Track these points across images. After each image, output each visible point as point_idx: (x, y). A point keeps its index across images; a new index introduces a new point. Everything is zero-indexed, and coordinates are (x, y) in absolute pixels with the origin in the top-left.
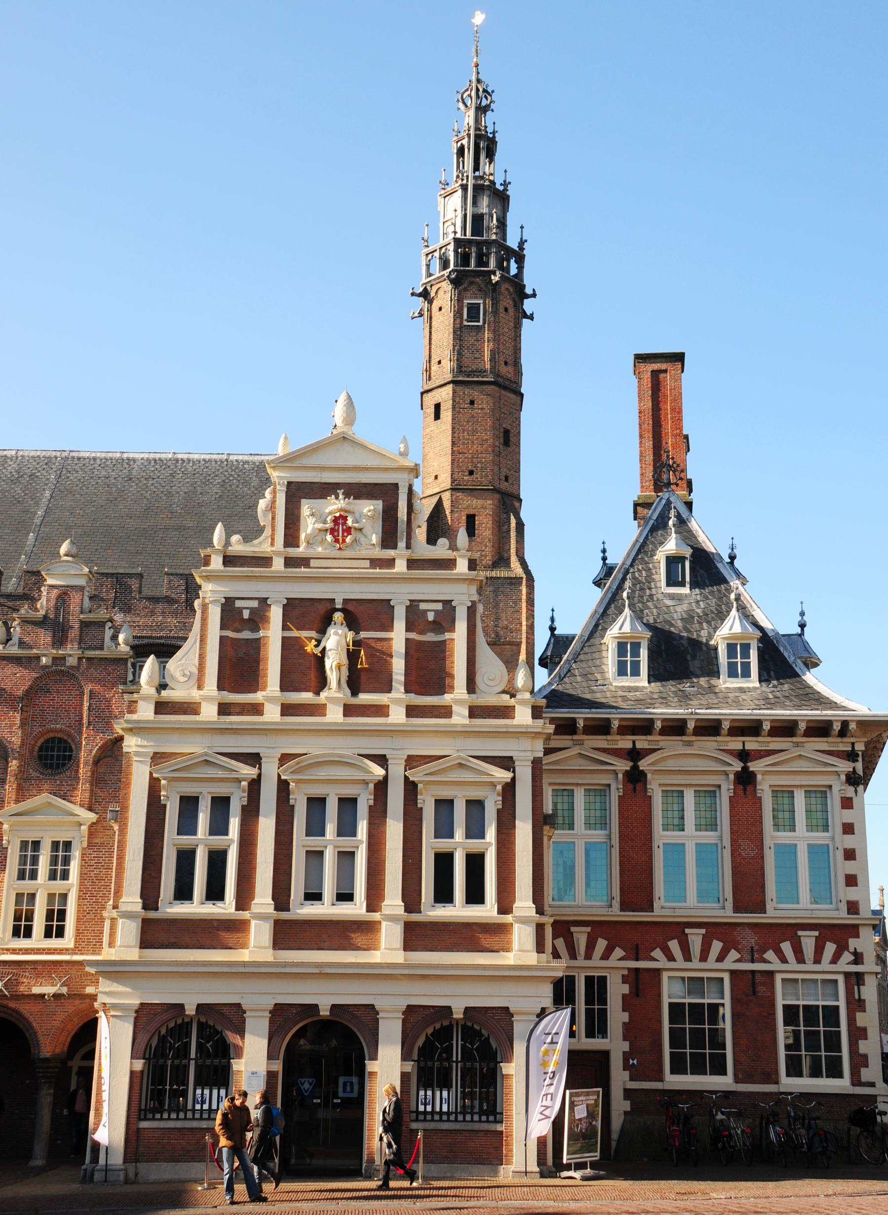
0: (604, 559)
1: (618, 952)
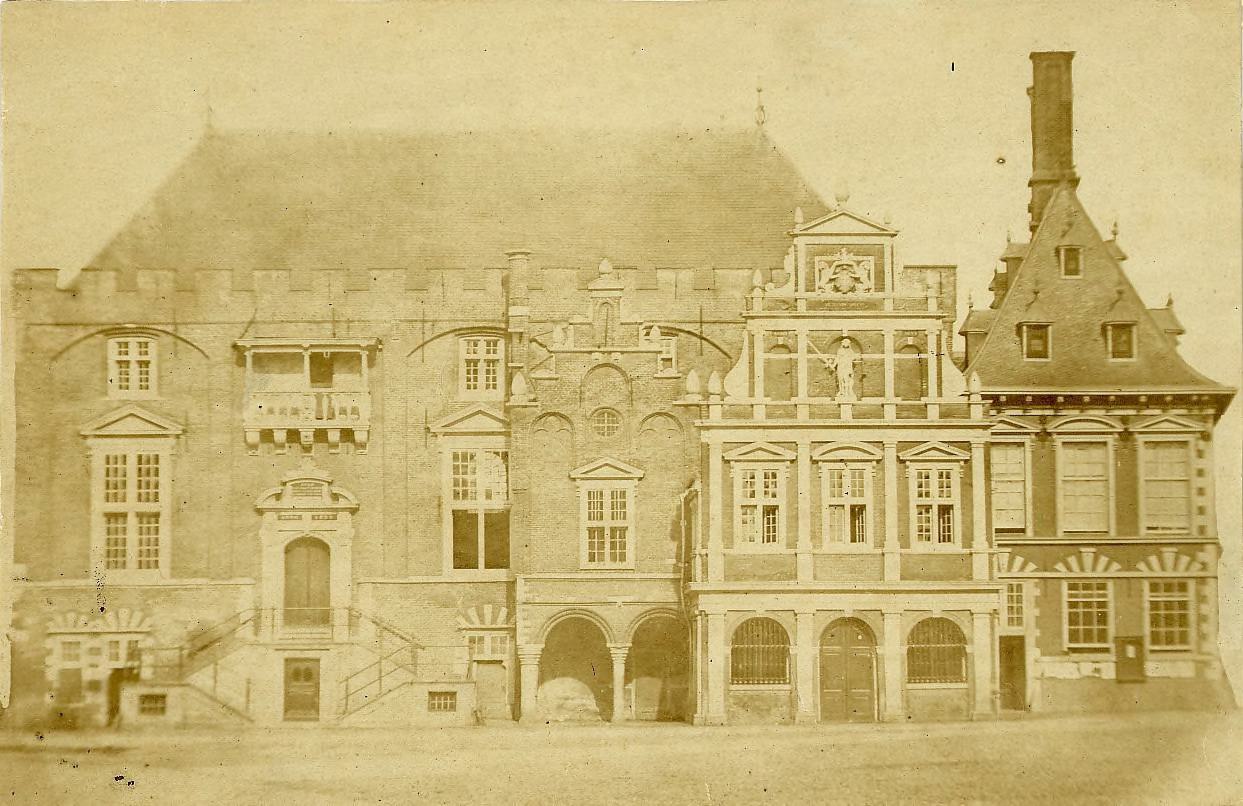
0: (1009, 241)
1: (1032, 566)
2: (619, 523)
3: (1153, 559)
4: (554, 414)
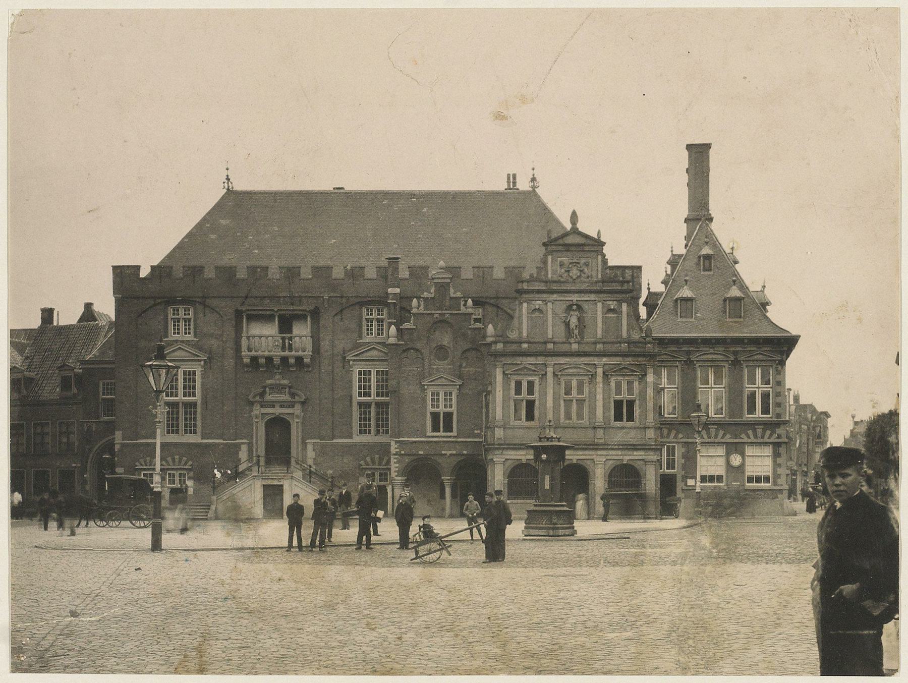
0: (672, 251)
1: (680, 436)
2: (448, 410)
3: (750, 432)
4: (412, 349)
